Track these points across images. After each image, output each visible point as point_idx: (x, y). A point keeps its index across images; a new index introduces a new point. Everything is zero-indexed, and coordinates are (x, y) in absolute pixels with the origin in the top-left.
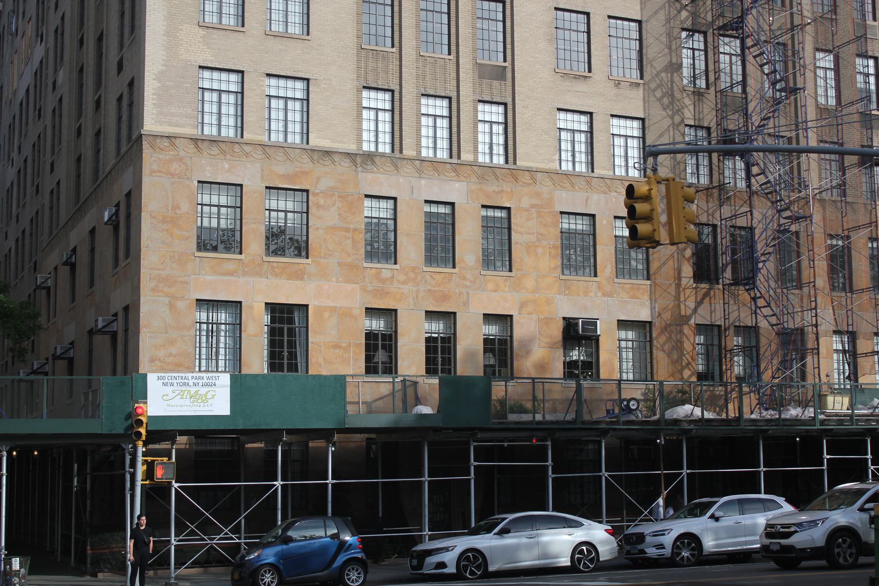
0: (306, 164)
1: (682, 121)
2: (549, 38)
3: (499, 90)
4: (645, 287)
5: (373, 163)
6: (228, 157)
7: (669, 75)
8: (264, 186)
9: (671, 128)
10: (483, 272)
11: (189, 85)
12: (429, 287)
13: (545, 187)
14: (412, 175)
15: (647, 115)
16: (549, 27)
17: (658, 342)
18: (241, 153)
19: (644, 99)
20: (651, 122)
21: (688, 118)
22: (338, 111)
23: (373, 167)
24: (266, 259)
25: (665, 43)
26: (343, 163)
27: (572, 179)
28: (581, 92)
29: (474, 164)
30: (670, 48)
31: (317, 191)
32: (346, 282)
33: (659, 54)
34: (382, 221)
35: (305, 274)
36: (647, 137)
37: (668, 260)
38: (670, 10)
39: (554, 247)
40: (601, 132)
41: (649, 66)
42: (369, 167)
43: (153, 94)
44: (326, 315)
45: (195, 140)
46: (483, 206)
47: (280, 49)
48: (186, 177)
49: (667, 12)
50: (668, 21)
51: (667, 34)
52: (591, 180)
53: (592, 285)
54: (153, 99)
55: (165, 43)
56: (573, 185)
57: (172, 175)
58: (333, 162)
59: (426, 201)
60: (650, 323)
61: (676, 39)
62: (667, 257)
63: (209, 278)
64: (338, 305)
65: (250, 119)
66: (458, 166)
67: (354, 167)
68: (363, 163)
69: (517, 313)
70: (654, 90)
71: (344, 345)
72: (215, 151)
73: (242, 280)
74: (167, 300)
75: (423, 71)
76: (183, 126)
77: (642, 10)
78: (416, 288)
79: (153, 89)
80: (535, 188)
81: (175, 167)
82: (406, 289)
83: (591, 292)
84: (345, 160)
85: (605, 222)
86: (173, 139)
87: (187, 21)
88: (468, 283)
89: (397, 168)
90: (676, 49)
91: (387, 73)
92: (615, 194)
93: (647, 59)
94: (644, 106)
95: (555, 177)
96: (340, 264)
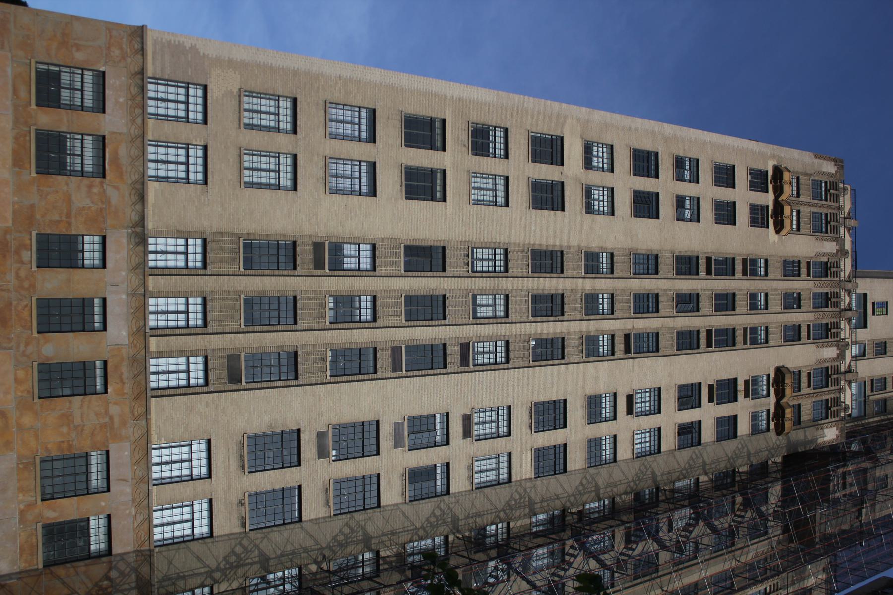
1: (217, 582)
2: (273, 425)
3: (219, 374)
4: (35, 562)
5: (138, 244)
6: (130, 102)
7: (257, 559)
8: (106, 133)
9: (207, 569)
10: (35, 365)
11: (190, 74)
12: (14, 303)
13: (132, 431)
14: (130, 285)
15: (217, 539)
19: (231, 534)
20: (211, 544)
21: (219, 587)
23: (134, 244)
24: (33, 128)
25: (285, 550)
26: (134, 213)
27: (144, 461)
28: (229, 464)
29: (147, 355)
30: (282, 555)
31: (105, 186)
32: (14, 212)
33: (275, 545)
34: (80, 255)
35: (20, 168)
36: (196, 542)
39: (70, 447)
40: (194, 490)
41: (263, 535)
42: (133, 240)
43: (179, 41)
45: (142, 72)
46: (105, 363)
47: (229, 159)
48: (107, 61)
49: (313, 547)
50: (306, 550)
51: (294, 550)
53: (32, 497)
54: (175, 41)
56: (138, 462)
57: (108, 48)
58: (134, 204)
59: (104, 300)
63: (9, 70)
66: (143, 333)
70: (240, 544)
72: (135, 90)
73: (9, 103)
76: (153, 64)
77: (311, 520)
78: (12, 289)
79: (183, 42)
82: (11, 277)
83: (24, 496)
84: (137, 216)
85: (103, 504)
88: (22, 348)
89: (135, 268)
91: (221, 261)
92: (134, 513)
93: (268, 532)
94: (225, 535)
95: (144, 442)
96: (33, 206)
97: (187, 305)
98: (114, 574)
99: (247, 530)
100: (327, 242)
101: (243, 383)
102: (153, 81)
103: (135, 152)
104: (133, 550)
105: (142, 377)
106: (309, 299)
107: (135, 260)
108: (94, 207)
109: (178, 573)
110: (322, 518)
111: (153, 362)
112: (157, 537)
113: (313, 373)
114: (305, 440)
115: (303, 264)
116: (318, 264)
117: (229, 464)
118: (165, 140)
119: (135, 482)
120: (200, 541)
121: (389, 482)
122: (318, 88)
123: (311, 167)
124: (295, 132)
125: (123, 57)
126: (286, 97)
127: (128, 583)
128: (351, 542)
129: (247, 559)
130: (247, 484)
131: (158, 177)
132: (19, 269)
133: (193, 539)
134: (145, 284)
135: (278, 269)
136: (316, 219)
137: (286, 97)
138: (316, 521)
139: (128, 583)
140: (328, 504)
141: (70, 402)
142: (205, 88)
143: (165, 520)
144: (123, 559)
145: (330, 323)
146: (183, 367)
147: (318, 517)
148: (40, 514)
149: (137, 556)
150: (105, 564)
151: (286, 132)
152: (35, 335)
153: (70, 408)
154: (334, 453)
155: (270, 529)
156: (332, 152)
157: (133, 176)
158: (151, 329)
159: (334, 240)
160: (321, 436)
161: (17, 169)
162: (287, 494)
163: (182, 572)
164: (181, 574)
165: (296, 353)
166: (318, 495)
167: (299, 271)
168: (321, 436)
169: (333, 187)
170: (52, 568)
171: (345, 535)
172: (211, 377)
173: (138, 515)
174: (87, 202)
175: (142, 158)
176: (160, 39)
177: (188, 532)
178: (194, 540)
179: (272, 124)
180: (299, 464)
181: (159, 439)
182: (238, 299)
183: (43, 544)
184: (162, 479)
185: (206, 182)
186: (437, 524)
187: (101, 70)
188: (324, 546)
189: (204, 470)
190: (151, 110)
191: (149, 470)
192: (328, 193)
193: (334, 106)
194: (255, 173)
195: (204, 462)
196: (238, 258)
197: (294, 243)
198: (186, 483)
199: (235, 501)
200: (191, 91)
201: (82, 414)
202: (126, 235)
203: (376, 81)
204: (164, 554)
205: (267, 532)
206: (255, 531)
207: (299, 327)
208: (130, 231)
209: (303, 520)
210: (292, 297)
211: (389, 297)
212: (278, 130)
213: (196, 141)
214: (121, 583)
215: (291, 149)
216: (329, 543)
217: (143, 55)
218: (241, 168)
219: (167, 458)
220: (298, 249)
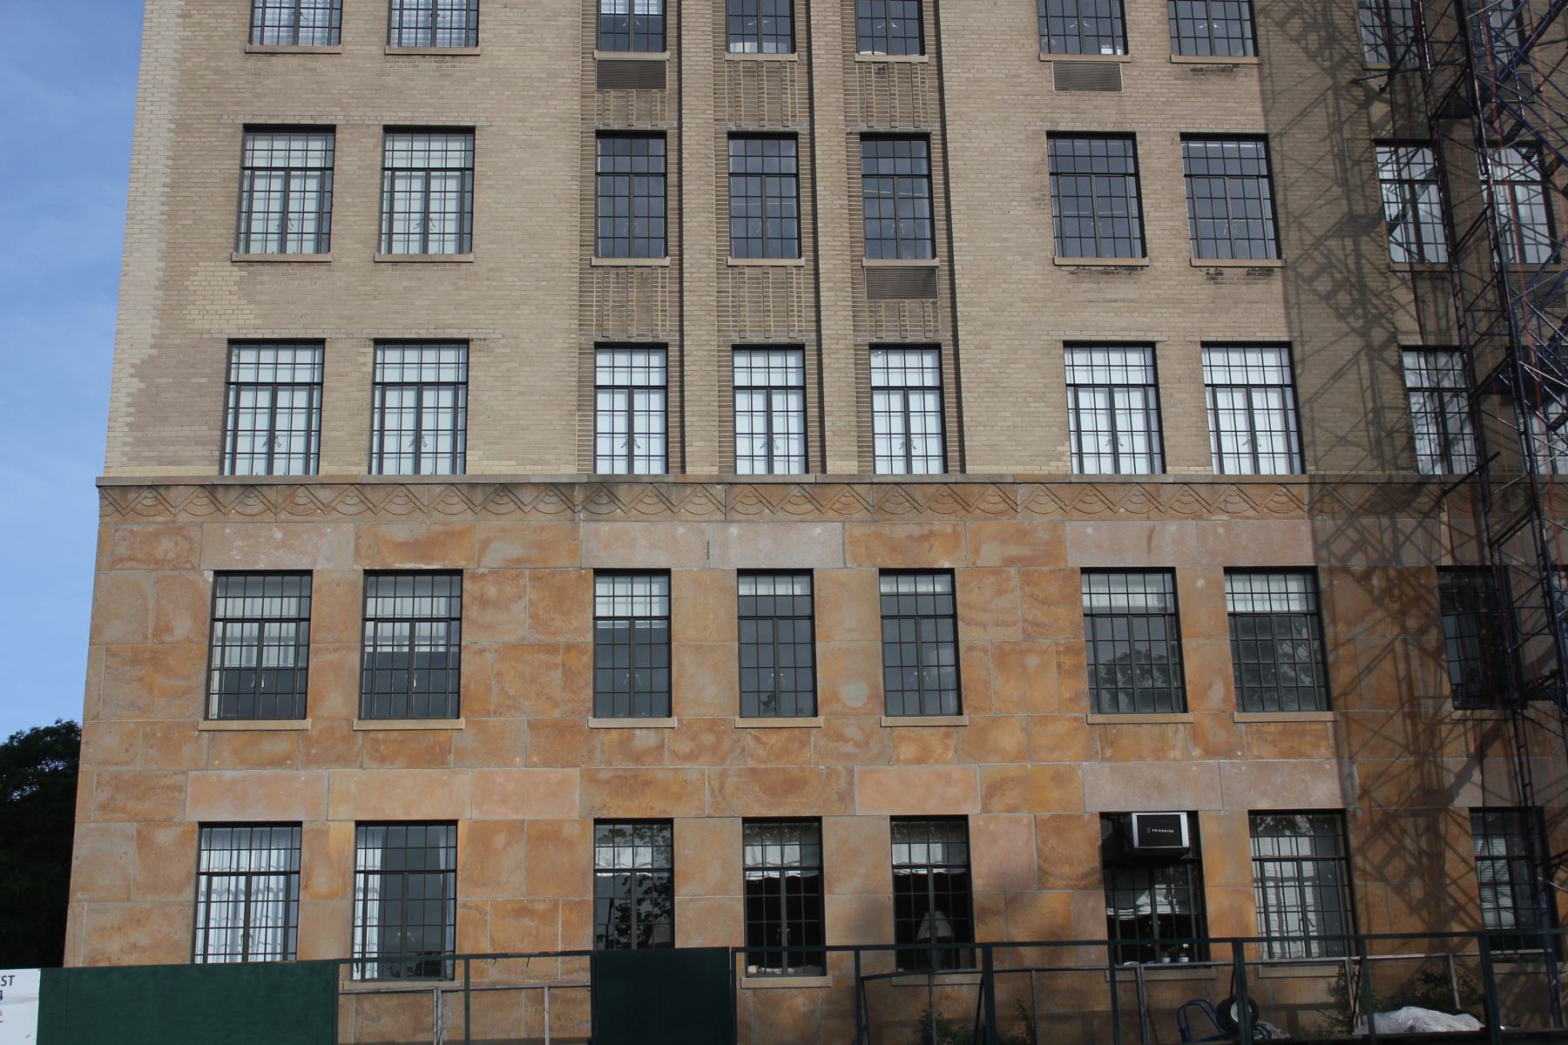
0: (458, 513)
1: (1393, 338)
2: (1037, 195)
3: (914, 319)
4: (1320, 727)
5: (613, 498)
6: (283, 516)
7: (1349, 242)
8: (360, 568)
9: (1363, 359)
10: (887, 721)
11: (205, 380)
12: (751, 764)
13: (1041, 517)
15: (1296, 334)
16: (1037, 173)
17: (1365, 858)
18: (311, 505)
19: (1286, 300)
20: (1306, 348)
21: (1408, 333)
22: (534, 398)
23: (613, 507)
26: (541, 507)
27: (1108, 492)
28: (1123, 300)
30: (1345, 183)
31: (481, 571)
32: (547, 764)
33: (1318, 199)
34: (640, 625)
35: (450, 752)
36: (1299, 382)
37: (1377, 660)
38: (1338, 104)
39: (1070, 650)
40: (1180, 382)
41: (1294, 228)
42: (604, 510)
43: (129, 405)
44: (500, 840)
45: (210, 488)
46: (884, 572)
48: (188, 566)
49: (1331, 110)
50: (1336, 127)
51: (1334, 155)
52: (1158, 490)
53: (1176, 732)
55: (159, 302)
56: (1111, 506)
57: (160, 564)
58: (520, 506)
59: (743, 573)
60: (1342, 812)
61: (1358, 163)
62: (1377, 652)
63: (229, 775)
64: (528, 817)
65: (334, 434)
66: (817, 489)
68: (590, 500)
69: (978, 810)
70: (1311, 279)
71: (540, 907)
72: (254, 505)
73: (303, 775)
74: (132, 828)
75: (733, 297)
76: (188, 463)
79: (130, 395)
80: (1013, 521)
81: (167, 547)
82: (694, 770)
83: (1173, 748)
84: (548, 499)
85: (1200, 583)
86: (162, 491)
87: (208, 255)
88: (849, 748)
89: (669, 505)
90: (1363, 184)
91: (649, 309)
92: (1225, 517)
93: (1288, 213)
94: (1288, 316)
95: (1065, 492)
96: (533, 726)
97: (751, 389)
98: (1358, 564)
99: (1279, 263)
100: (597, 55)
101: (936, 262)
102: (227, 463)
103: (399, 505)
104: (1308, 522)
105: (917, 492)
106: (735, 103)
107: (651, 504)
108: (531, 594)
109: (1367, 423)
110: (1261, 86)
111: (882, 468)
112: (1282, 468)
113: (914, 97)
115: (650, 115)
116: (651, 77)
118: (366, 437)
119: (1154, 513)
120: (1298, 372)
122: (216, 71)
123: (415, 92)
124: (329, 130)
125: (179, 531)
126: (244, 150)
127: (1382, 533)
128: (1324, 16)
129: (1346, 266)
130: (1172, 260)
131: (454, 453)
132: (674, 753)
134: (704, 484)
135: (665, 175)
136: (540, 80)
137: (244, 150)
138: (1268, 100)
139: (1382, 533)
140: (1229, 70)
141: (971, 648)
142: (236, 343)
143: (1245, 448)
144: (1326, 544)
145: (793, 51)
146: (896, 401)
147: (1258, 96)
148: (1216, 715)
149: (1321, 511)
150: (1335, 582)
151: (331, 151)
152: (820, 720)
153: (984, 650)
154: (1106, 51)
155: (1280, 210)
156: (376, 39)
157: (455, 509)
158: (807, 471)
159: (592, 39)
160: (1067, 80)
161: (451, 757)
162: (1199, 168)
163: (1366, 414)
164: (1370, 416)
165: (865, 137)
167: (667, 124)
168: (1067, 80)
169: (459, 39)
170: (1335, 691)
171: (1307, 29)
172: (920, 338)
173: (1230, 508)
174: (520, 609)
175: (412, 488)
176: (127, 449)
177: (1274, 399)
178: (1293, 386)
179: (312, 184)
180: (1131, 136)
181: (1059, 456)
182: (736, 270)
183: (1281, 709)
184: (1150, 453)
185: (463, 343)
187: (211, 580)
188: (1329, 82)
189: (1135, 357)
190: (297, 468)
191: (1129, 482)
192: (477, 51)
193: (257, 32)
194: (435, 227)
195: (1116, 357)
196: (640, 270)
197: (600, 134)
198: (1162, 400)
199: (1210, 289)
200: (247, 376)
201: (997, 625)
202: (593, 524)
204: (1321, 454)
205: (1287, 217)
206: (1284, 245)
207: (802, 128)
209: (1263, 131)
210: (732, 143)
212: (327, 170)
213: (364, 364)
214: (1380, 548)
215: (375, 140)
216: (1323, 69)
217: (168, 486)
218: (424, 260)
219: (1104, 440)
220: (616, 126)
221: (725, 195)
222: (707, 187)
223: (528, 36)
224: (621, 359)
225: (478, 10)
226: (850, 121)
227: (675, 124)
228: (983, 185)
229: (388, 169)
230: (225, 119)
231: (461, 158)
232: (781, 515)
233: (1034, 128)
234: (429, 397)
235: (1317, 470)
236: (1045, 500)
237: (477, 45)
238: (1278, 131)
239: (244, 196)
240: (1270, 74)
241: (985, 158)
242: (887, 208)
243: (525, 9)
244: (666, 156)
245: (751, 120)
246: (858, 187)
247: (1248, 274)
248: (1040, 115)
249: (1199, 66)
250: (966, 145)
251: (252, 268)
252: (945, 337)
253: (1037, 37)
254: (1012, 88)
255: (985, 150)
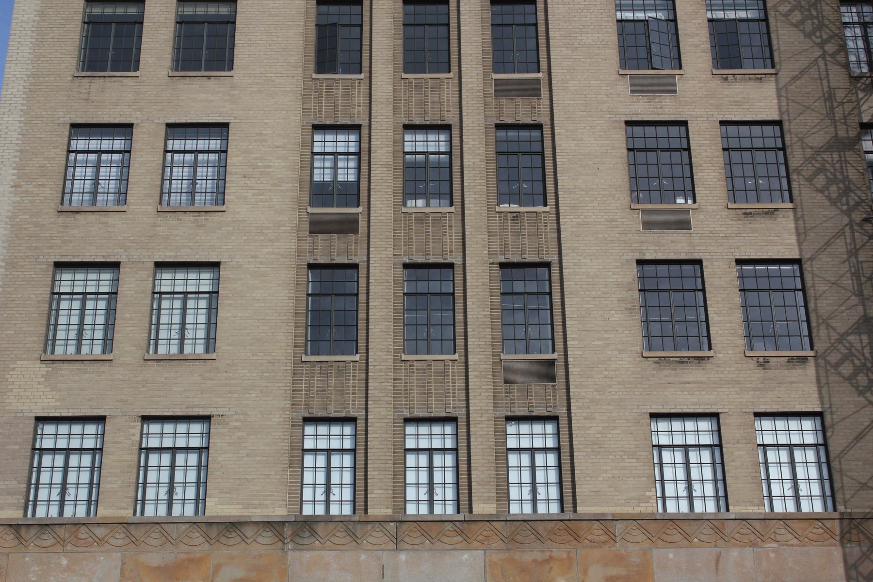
2: (629, 306)
5: (313, 533)
6: (69, 547)
11: (17, 447)
14: (382, 547)
15: (827, 406)
16: (629, 290)
18: (90, 539)
19: (818, 381)
20: (835, 416)
22: (257, 459)
23: (313, 539)
25: (851, 288)
26: (260, 539)
27: (685, 526)
28: (694, 383)
30: (860, 294)
33: (841, 306)
36: (830, 442)
38: (853, 236)
40: (738, 443)
42: (306, 541)
47: (166, 379)
49: (848, 241)
50: (853, 252)
51: (852, 274)
52: (723, 525)
56: (687, 537)
58: (244, 539)
65: (109, 486)
66: (465, 525)
67: (280, 543)
68: (296, 534)
72: (48, 539)
75: (405, 383)
77: (800, 243)
80: (613, 549)
84: (265, 534)
87: (24, 356)
92: (775, 545)
93: (818, 317)
95: (652, 526)
97: (417, 451)
99: (812, 353)
100: (311, 210)
103: (155, 538)
104: (840, 548)
105: (540, 527)
106: (409, 243)
107: (341, 537)
110: (796, 224)
111: (515, 509)
112: (818, 507)
113: (539, 236)
114: (656, 252)
115: (347, 252)
116: (348, 225)
117: (694, 383)
118: (133, 488)
120: (829, 434)
121: (737, 103)
123: (178, 238)
124: (115, 265)
126: (54, 280)
128: (842, 173)
129: (863, 354)
130: (730, 352)
131: (197, 500)
133: (823, 446)
134: (381, 522)
135: (357, 295)
136: (268, 228)
137: (54, 280)
138: (801, 235)
140: (771, 213)
142: (41, 420)
143: (789, 493)
144: (855, 566)
145: (451, 205)
147: (794, 231)
149: (850, 541)
151: (116, 281)
154: (680, 201)
155: (812, 315)
156: (151, 201)
158: (458, 512)
159: (306, 198)
160: (650, 223)
165: (503, 266)
166: (754, 231)
167: (359, 258)
168: (650, 223)
169: (212, 200)
171: (830, 182)
172: (543, 412)
173: (779, 538)
177: (811, 455)
178: (825, 445)
179: (102, 305)
180: (699, 262)
181: (647, 500)
182: (408, 364)
184: (717, 497)
185: (205, 419)
186: (817, 18)
188: (846, 220)
189: (704, 425)
190: (81, 512)
191: (700, 519)
193: (67, 197)
194: (189, 334)
196: (337, 364)
197: (311, 266)
198: (725, 456)
199: (760, 373)
200: (48, 443)
202: (298, 553)
203: (20, 122)
204: (848, 496)
205: (817, 320)
206: (815, 340)
207: (457, 260)
208: (290, 546)
209: (798, 257)
210: (406, 272)
211: (407, 101)
212: (113, 295)
213: (134, 435)
215: (147, 272)
216: (842, 211)
218: (181, 359)
219: (682, 487)
220: (322, 260)
221: (401, 309)
222: (387, 304)
223: (260, 197)
224: (323, 429)
225: (225, 180)
226: (492, 254)
227: (365, 259)
228: (588, 299)
229: (157, 293)
230: (41, 259)
231: (210, 285)
232: (439, 545)
233: (627, 257)
234: (180, 459)
235: (846, 508)
236: (637, 532)
237: (224, 204)
238: (809, 257)
239: (53, 312)
240: (803, 216)
241: (591, 280)
242: (520, 317)
243: (259, 178)
244: (358, 282)
245: (420, 255)
246: (498, 302)
247: (788, 362)
248: (631, 248)
249: (749, 211)
250: (576, 270)
251: (55, 365)
252: (562, 411)
253: (629, 192)
254: (610, 229)
255: (592, 274)
